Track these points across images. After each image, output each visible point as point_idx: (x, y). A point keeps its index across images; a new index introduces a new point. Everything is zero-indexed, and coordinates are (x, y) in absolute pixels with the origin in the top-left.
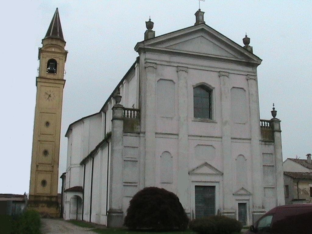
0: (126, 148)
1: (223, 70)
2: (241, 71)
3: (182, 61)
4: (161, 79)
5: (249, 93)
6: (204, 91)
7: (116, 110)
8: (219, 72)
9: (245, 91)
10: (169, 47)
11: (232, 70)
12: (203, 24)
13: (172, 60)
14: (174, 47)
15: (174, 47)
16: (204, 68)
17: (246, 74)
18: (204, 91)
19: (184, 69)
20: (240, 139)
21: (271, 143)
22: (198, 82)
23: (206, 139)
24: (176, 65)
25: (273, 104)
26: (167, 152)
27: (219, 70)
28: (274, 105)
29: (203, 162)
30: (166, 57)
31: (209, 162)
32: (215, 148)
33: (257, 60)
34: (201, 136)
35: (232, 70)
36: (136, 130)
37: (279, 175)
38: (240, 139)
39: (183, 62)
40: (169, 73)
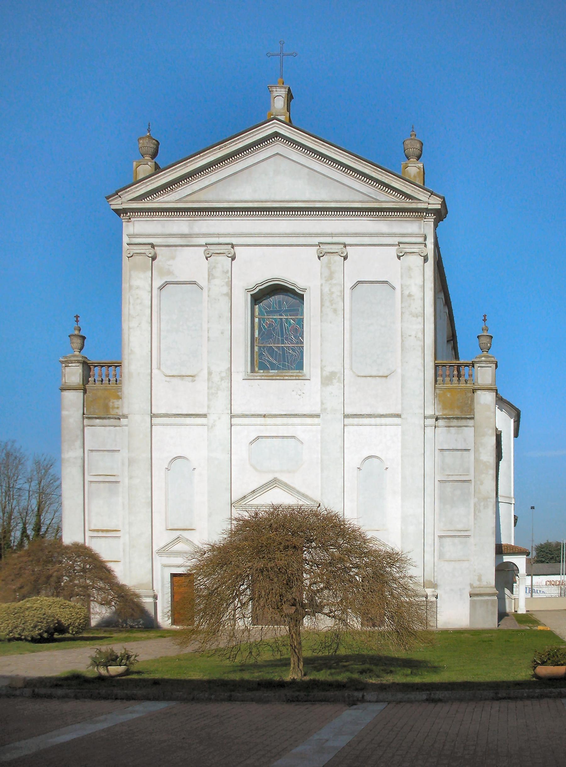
0: (94, 453)
1: (329, 240)
2: (382, 235)
3: (212, 230)
4: (167, 283)
5: (402, 294)
6: (276, 302)
7: (67, 369)
8: (320, 244)
9: (394, 288)
10: (189, 198)
11: (356, 235)
12: (275, 121)
13: (196, 230)
14: (202, 196)
15: (202, 196)
16: (366, 240)
17: (396, 240)
18: (276, 302)
19: (335, 248)
20: (370, 416)
21: (463, 422)
22: (260, 279)
23: (279, 420)
24: (203, 241)
25: (485, 316)
26: (175, 458)
27: (316, 240)
28: (485, 320)
29: (270, 477)
30: (180, 225)
31: (284, 478)
32: (302, 443)
33: (427, 200)
34: (264, 416)
35: (356, 235)
36: (113, 412)
37: (482, 504)
38: (370, 416)
39: (222, 231)
40: (188, 263)
